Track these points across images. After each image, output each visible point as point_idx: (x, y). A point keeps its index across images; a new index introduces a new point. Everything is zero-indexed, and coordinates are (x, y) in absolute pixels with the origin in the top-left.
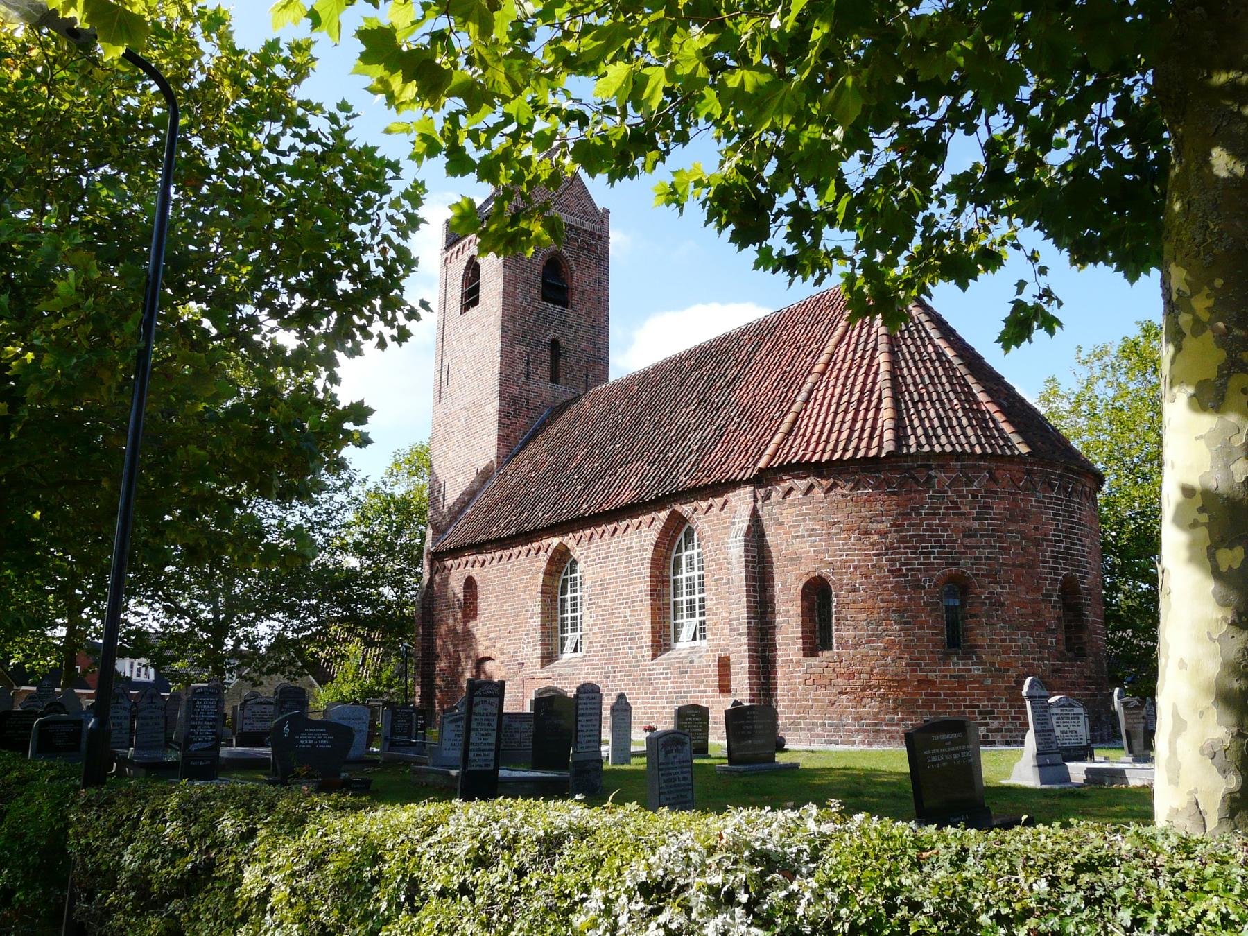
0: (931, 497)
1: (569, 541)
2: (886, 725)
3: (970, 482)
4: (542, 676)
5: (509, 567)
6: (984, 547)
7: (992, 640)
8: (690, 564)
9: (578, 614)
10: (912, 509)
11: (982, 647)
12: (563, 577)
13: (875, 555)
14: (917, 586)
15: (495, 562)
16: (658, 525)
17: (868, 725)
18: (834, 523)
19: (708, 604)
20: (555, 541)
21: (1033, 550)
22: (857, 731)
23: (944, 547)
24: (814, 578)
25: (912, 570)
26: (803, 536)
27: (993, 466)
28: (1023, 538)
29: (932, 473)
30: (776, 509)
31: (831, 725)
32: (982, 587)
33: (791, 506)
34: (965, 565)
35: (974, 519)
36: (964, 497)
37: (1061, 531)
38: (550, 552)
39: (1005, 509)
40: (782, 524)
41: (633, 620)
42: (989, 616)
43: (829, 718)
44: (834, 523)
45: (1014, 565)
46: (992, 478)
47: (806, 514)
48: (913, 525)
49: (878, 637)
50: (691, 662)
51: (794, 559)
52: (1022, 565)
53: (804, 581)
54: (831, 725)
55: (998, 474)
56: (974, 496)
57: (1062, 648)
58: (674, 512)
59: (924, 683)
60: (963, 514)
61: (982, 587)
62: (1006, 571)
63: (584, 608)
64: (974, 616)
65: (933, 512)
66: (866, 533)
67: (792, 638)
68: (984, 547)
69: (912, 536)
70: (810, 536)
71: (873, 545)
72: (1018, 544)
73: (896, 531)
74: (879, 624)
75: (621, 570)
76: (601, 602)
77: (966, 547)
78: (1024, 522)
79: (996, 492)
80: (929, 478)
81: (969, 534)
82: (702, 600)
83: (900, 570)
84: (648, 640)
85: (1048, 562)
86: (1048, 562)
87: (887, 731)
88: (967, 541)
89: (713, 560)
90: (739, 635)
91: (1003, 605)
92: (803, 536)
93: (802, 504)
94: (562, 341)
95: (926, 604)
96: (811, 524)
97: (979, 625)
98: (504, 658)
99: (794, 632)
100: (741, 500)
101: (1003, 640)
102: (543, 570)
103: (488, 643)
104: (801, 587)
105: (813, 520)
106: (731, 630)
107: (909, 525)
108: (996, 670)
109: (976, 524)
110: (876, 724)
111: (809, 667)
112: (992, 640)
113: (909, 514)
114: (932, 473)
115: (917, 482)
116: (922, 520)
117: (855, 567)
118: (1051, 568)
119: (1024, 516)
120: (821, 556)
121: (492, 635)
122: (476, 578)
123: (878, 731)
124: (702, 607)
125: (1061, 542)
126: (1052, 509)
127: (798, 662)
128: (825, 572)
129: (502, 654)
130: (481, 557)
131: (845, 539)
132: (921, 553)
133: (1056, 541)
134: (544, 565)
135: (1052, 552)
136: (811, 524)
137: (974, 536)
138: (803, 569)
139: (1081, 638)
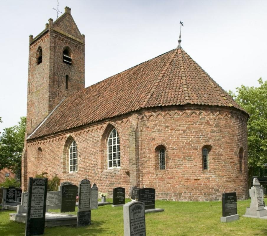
1: (73, 135)
2: (183, 194)
4: (64, 178)
5: (52, 144)
8: (115, 142)
9: (76, 159)
10: (194, 123)
12: (71, 147)
13: (181, 138)
14: (195, 149)
15: (48, 143)
16: (104, 129)
17: (177, 194)
18: (167, 127)
20: (68, 135)
22: (173, 196)
23: (204, 136)
24: (159, 146)
25: (194, 143)
26: (156, 131)
27: (221, 109)
30: (146, 123)
31: (164, 194)
32: (216, 149)
33: (151, 121)
35: (215, 127)
38: (66, 139)
39: (224, 124)
40: (148, 127)
41: (95, 160)
43: (164, 192)
44: (167, 127)
47: (157, 124)
48: (194, 128)
49: (181, 165)
50: (115, 173)
51: (153, 139)
53: (156, 147)
54: (164, 194)
56: (215, 119)
58: (109, 125)
60: (210, 125)
63: (78, 156)
65: (201, 124)
66: (178, 130)
67: (151, 165)
69: (194, 132)
70: (158, 131)
71: (180, 134)
73: (188, 130)
74: (182, 161)
75: (91, 144)
76: (84, 154)
80: (200, 114)
81: (212, 132)
82: (119, 153)
83: (190, 143)
85: (236, 142)
87: (184, 196)
88: (212, 134)
89: (123, 140)
90: (134, 164)
91: (222, 155)
92: (156, 131)
93: (156, 121)
96: (158, 128)
98: (51, 173)
99: (152, 163)
100: (133, 120)
102: (64, 145)
103: (46, 168)
104: (155, 148)
105: (160, 126)
106: (130, 163)
108: (220, 177)
109: (215, 129)
110: (180, 194)
111: (157, 175)
113: (193, 124)
115: (196, 114)
117: (174, 142)
118: (237, 144)
120: (162, 138)
121: (47, 166)
122: (41, 148)
123: (181, 196)
124: (119, 156)
125: (240, 136)
126: (238, 125)
127: (153, 173)
128: (163, 143)
129: (51, 172)
130: (43, 141)
131: (170, 132)
132: (197, 138)
133: (239, 136)
134: (64, 143)
135: (237, 139)
136: (158, 128)
138: (155, 142)
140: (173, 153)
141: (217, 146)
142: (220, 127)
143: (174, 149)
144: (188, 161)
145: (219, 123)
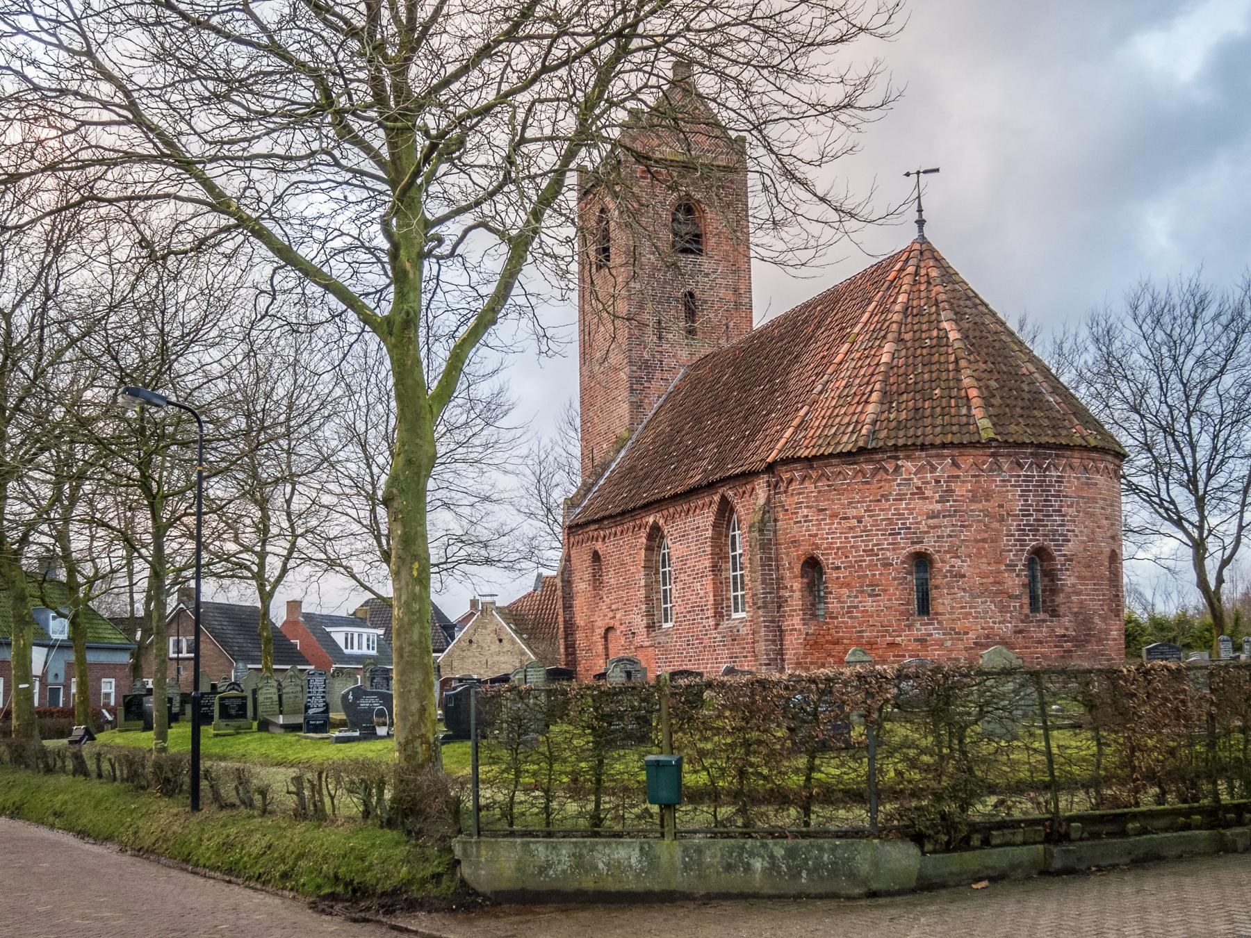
0: (899, 485)
3: (933, 469)
6: (946, 527)
7: (952, 608)
10: (882, 496)
11: (942, 614)
14: (887, 565)
19: (746, 579)
21: (996, 525)
27: (956, 452)
28: (985, 516)
29: (900, 463)
32: (943, 561)
34: (929, 545)
35: (937, 502)
36: (928, 483)
37: (1031, 505)
42: (950, 587)
45: (977, 541)
46: (955, 464)
52: (984, 540)
55: (960, 460)
56: (938, 482)
57: (1027, 611)
59: (892, 645)
60: (927, 498)
61: (943, 561)
62: (967, 547)
64: (937, 587)
65: (900, 499)
66: (845, 518)
68: (946, 527)
69: (883, 520)
71: (851, 528)
72: (979, 521)
77: (929, 527)
78: (987, 500)
79: (958, 477)
80: (897, 468)
84: (710, 613)
85: (1013, 535)
86: (1013, 535)
88: (931, 522)
91: (964, 576)
94: (697, 294)
95: (894, 579)
97: (941, 595)
101: (962, 608)
107: (881, 510)
108: (956, 633)
109: (939, 507)
112: (952, 608)
114: (900, 463)
115: (886, 471)
116: (891, 506)
117: (838, 548)
119: (988, 496)
137: (938, 517)
139: (1053, 601)
140: (838, 578)
141: (946, 552)
142: (954, 501)
143: (838, 568)
144: (870, 596)
145: (950, 491)
